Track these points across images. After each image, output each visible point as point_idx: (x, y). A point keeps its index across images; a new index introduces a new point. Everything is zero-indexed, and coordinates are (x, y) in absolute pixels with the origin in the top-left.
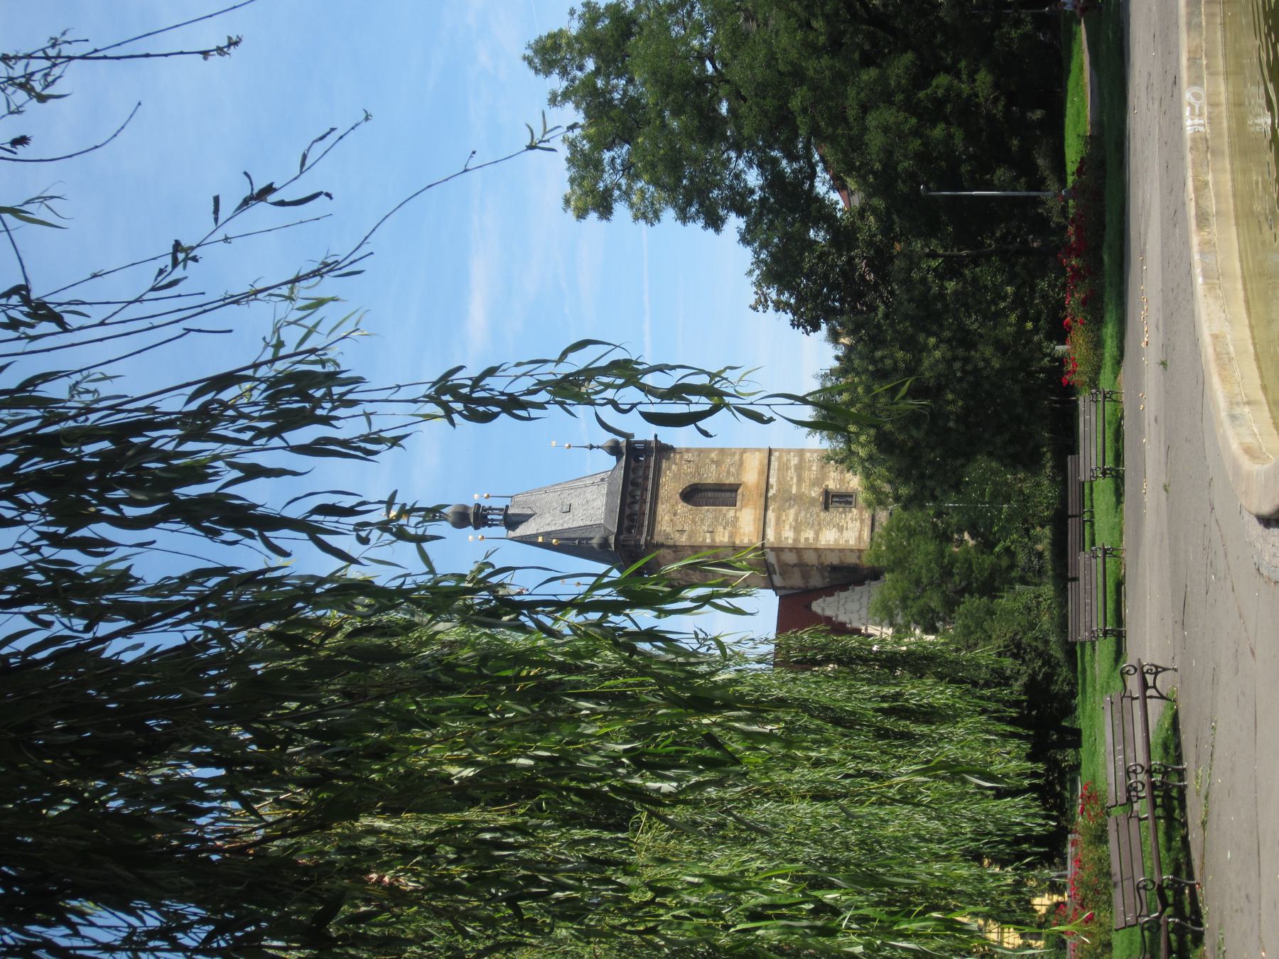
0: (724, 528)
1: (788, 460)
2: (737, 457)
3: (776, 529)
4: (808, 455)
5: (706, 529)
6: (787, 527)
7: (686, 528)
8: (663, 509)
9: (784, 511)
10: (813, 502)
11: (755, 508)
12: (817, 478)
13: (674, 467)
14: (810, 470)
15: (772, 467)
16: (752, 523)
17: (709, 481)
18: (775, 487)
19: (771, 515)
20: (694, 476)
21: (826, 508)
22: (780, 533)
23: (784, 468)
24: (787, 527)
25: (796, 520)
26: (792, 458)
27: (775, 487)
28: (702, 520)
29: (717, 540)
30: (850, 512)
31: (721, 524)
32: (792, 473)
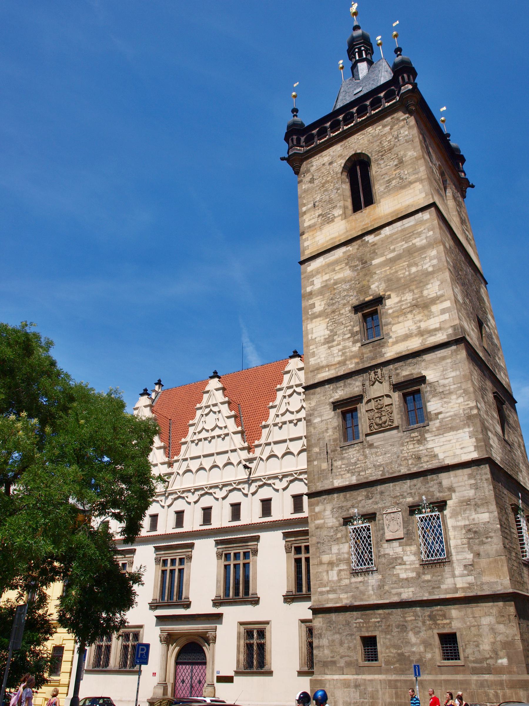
0: (319, 216)
1: (419, 234)
2: (412, 178)
3: (322, 266)
4: (434, 253)
7: (316, 182)
8: (337, 149)
9: (347, 264)
10: (364, 290)
11: (347, 231)
12: (399, 279)
14: (409, 266)
15: (405, 221)
16: (328, 238)
19: (339, 253)
21: (357, 309)
22: (319, 273)
23: (408, 235)
24: (326, 277)
25: (336, 283)
26: (423, 236)
27: (378, 238)
29: (305, 217)
30: (355, 342)
31: (323, 211)
32: (401, 246)
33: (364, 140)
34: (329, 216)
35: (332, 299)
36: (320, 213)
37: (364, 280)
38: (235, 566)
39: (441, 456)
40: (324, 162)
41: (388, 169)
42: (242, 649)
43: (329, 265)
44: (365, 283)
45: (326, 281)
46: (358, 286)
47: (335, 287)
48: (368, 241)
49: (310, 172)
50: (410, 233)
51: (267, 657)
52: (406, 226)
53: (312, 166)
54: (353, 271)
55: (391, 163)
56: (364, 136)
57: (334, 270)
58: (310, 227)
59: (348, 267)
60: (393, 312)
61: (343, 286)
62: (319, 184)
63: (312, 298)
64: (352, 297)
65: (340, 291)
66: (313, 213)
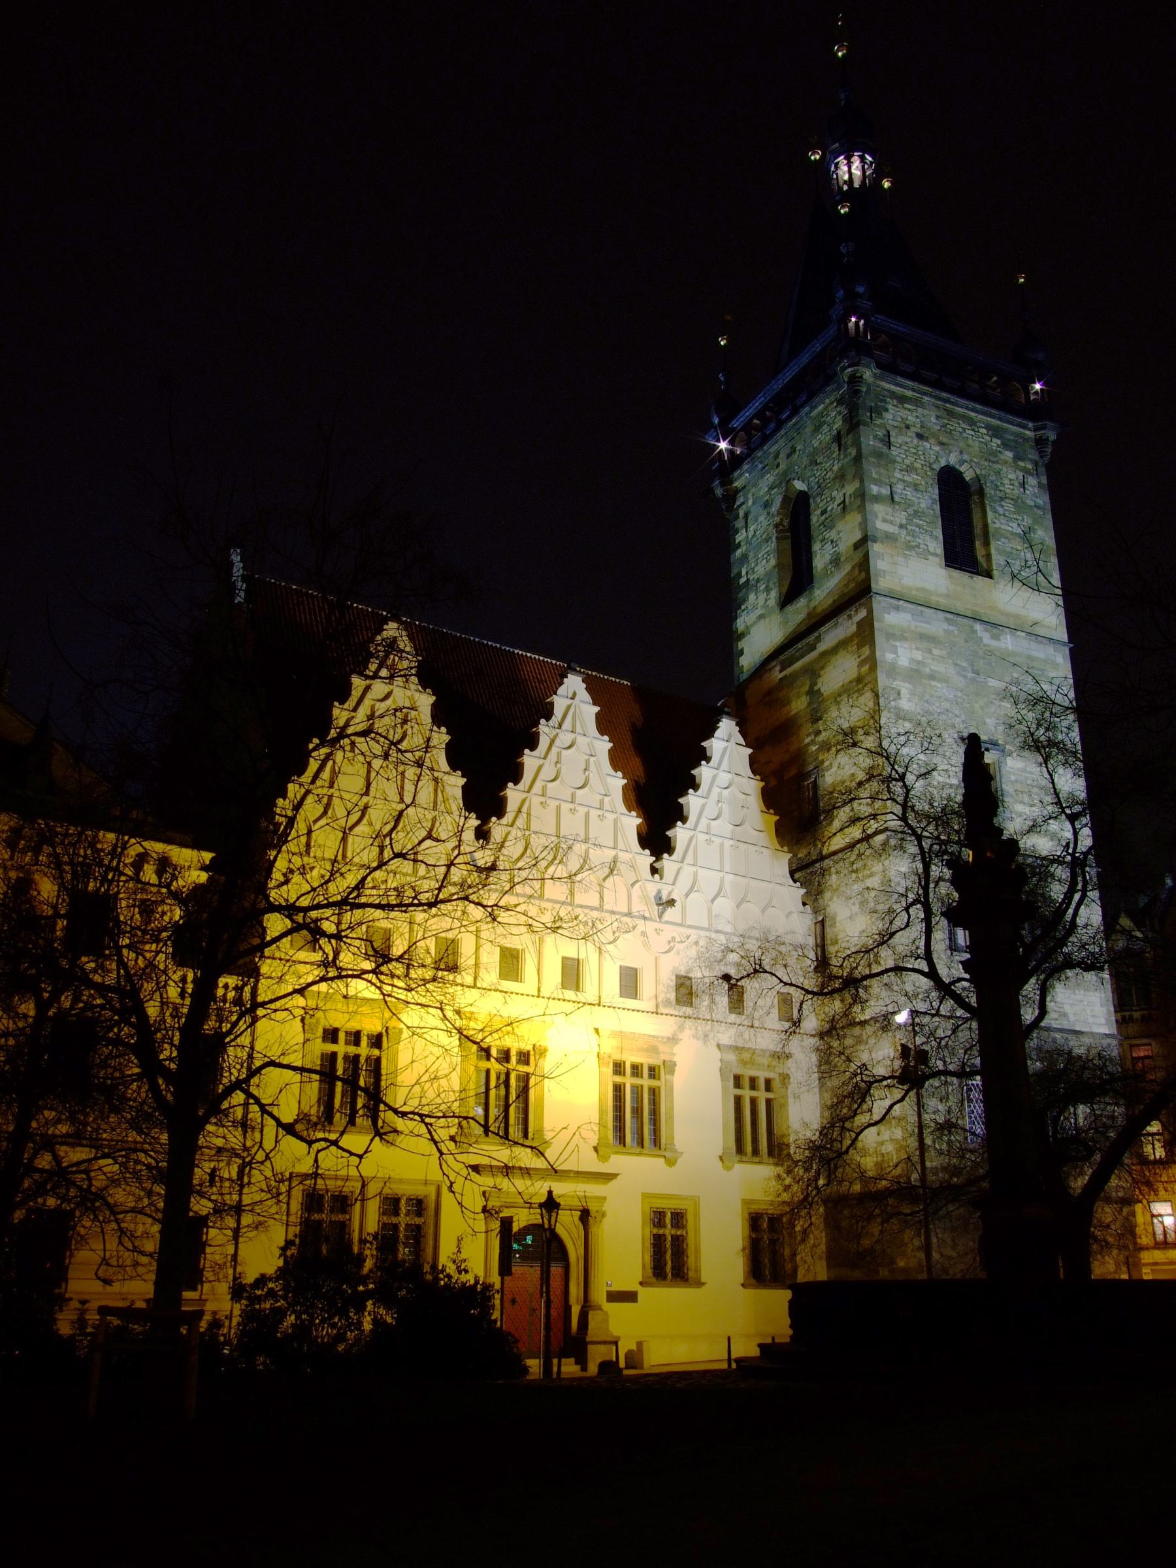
0: (901, 526)
5: (899, 488)
6: (918, 656)
11: (948, 596)
13: (1009, 455)
17: (990, 516)
18: (994, 643)
19: (937, 626)
20: (996, 487)
22: (906, 639)
24: (918, 656)
25: (932, 677)
27: (994, 643)
28: (915, 487)
31: (909, 520)
33: (974, 441)
34: (920, 541)
35: (927, 702)
36: (904, 522)
37: (976, 702)
38: (753, 1101)
39: (1072, 1018)
40: (908, 422)
41: (1012, 533)
42: (648, 1244)
43: (922, 637)
44: (977, 707)
45: (919, 662)
46: (968, 706)
47: (933, 683)
48: (981, 638)
49: (883, 419)
50: (1038, 669)
51: (691, 1261)
52: (1034, 653)
53: (887, 410)
54: (958, 674)
55: (1015, 525)
56: (973, 433)
57: (930, 651)
58: (889, 538)
59: (951, 661)
60: (1016, 781)
61: (944, 691)
62: (900, 460)
63: (895, 679)
64: (958, 719)
65: (940, 697)
66: (890, 510)
